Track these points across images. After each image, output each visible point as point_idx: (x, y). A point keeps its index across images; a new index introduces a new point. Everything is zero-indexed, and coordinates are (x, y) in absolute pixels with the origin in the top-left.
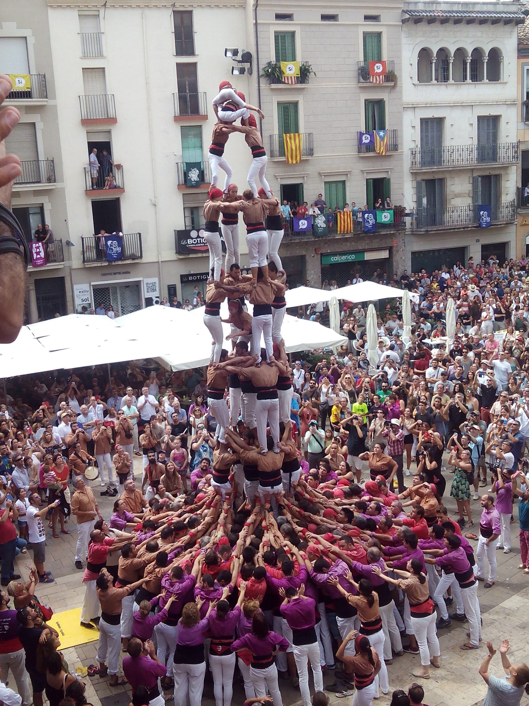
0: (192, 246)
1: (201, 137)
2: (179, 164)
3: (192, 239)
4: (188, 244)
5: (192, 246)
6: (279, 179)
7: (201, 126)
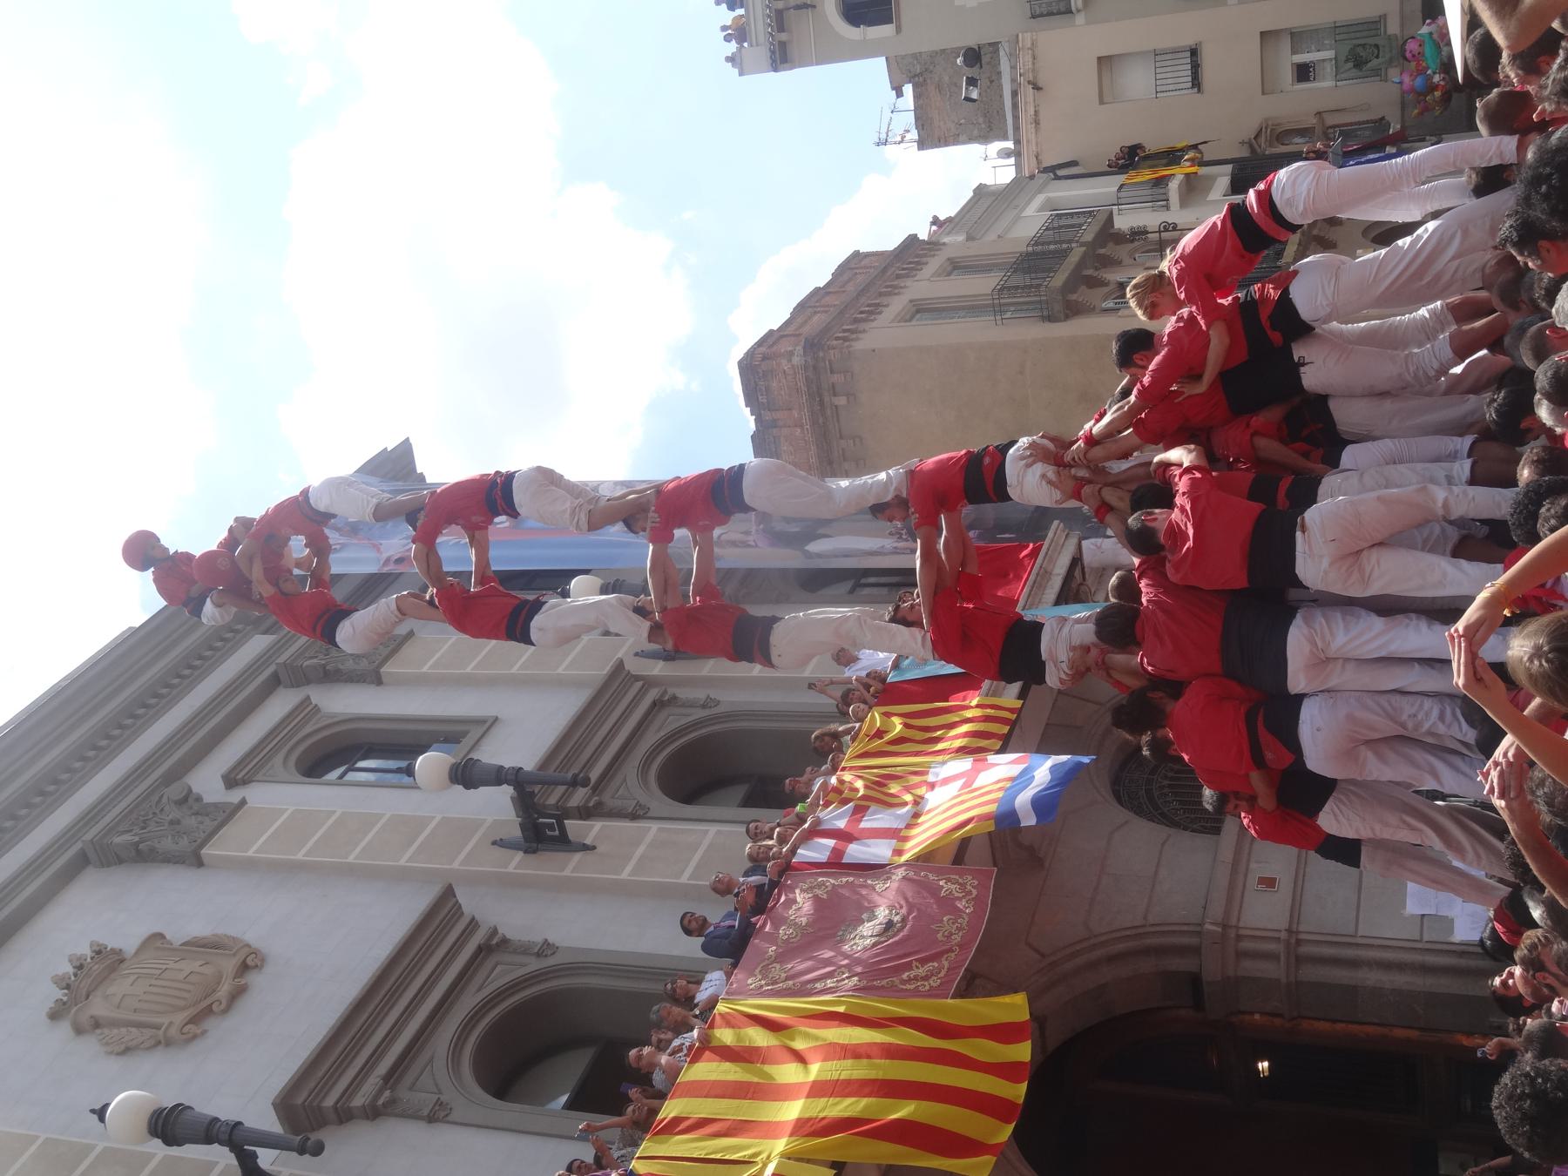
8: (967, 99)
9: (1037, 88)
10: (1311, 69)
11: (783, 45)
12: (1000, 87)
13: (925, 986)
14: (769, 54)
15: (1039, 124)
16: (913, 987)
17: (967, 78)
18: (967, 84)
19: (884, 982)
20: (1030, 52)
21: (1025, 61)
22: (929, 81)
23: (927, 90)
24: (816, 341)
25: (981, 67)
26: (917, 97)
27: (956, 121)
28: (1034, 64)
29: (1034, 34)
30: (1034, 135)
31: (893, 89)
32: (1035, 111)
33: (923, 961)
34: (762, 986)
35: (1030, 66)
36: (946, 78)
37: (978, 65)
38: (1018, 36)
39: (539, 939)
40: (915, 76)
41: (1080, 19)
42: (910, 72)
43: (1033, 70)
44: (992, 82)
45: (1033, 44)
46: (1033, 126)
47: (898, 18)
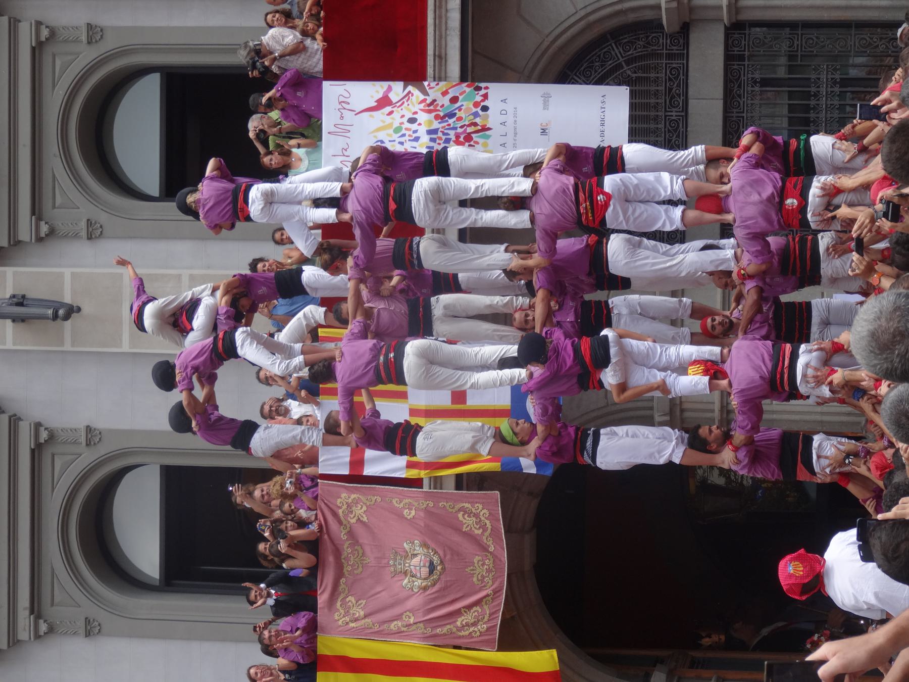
13: (476, 632)
16: (467, 633)
19: (445, 630)
33: (469, 607)
34: (347, 623)
39: (81, 425)
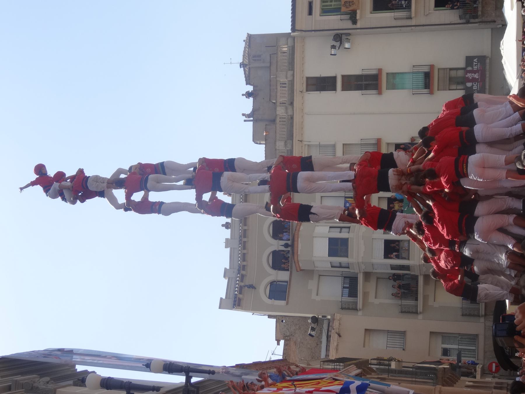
0: (479, 86)
1: (396, 73)
2: (413, 93)
3: (473, 85)
4: (477, 90)
5: (479, 86)
6: (430, 12)
7: (387, 74)
8: (310, 335)
9: (339, 336)
10: (449, 351)
11: (240, 300)
12: (321, 347)
14: (233, 302)
15: (338, 350)
17: (312, 327)
18: (311, 329)
20: (338, 321)
21: (336, 324)
22: (291, 339)
23: (290, 343)
24: (245, 367)
25: (318, 324)
26: (285, 345)
27: (300, 358)
28: (339, 326)
29: (341, 315)
30: (335, 354)
31: (276, 340)
32: (337, 345)
35: (338, 327)
36: (299, 340)
37: (317, 323)
38: (335, 314)
40: (286, 337)
41: (360, 313)
42: (285, 334)
43: (338, 329)
44: (317, 345)
45: (340, 319)
46: (335, 350)
47: (288, 298)
